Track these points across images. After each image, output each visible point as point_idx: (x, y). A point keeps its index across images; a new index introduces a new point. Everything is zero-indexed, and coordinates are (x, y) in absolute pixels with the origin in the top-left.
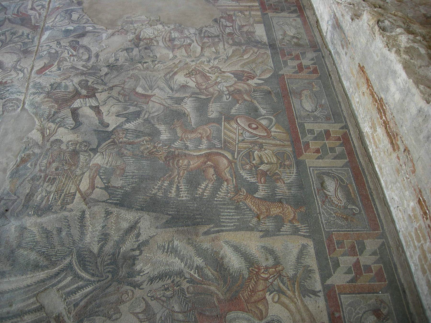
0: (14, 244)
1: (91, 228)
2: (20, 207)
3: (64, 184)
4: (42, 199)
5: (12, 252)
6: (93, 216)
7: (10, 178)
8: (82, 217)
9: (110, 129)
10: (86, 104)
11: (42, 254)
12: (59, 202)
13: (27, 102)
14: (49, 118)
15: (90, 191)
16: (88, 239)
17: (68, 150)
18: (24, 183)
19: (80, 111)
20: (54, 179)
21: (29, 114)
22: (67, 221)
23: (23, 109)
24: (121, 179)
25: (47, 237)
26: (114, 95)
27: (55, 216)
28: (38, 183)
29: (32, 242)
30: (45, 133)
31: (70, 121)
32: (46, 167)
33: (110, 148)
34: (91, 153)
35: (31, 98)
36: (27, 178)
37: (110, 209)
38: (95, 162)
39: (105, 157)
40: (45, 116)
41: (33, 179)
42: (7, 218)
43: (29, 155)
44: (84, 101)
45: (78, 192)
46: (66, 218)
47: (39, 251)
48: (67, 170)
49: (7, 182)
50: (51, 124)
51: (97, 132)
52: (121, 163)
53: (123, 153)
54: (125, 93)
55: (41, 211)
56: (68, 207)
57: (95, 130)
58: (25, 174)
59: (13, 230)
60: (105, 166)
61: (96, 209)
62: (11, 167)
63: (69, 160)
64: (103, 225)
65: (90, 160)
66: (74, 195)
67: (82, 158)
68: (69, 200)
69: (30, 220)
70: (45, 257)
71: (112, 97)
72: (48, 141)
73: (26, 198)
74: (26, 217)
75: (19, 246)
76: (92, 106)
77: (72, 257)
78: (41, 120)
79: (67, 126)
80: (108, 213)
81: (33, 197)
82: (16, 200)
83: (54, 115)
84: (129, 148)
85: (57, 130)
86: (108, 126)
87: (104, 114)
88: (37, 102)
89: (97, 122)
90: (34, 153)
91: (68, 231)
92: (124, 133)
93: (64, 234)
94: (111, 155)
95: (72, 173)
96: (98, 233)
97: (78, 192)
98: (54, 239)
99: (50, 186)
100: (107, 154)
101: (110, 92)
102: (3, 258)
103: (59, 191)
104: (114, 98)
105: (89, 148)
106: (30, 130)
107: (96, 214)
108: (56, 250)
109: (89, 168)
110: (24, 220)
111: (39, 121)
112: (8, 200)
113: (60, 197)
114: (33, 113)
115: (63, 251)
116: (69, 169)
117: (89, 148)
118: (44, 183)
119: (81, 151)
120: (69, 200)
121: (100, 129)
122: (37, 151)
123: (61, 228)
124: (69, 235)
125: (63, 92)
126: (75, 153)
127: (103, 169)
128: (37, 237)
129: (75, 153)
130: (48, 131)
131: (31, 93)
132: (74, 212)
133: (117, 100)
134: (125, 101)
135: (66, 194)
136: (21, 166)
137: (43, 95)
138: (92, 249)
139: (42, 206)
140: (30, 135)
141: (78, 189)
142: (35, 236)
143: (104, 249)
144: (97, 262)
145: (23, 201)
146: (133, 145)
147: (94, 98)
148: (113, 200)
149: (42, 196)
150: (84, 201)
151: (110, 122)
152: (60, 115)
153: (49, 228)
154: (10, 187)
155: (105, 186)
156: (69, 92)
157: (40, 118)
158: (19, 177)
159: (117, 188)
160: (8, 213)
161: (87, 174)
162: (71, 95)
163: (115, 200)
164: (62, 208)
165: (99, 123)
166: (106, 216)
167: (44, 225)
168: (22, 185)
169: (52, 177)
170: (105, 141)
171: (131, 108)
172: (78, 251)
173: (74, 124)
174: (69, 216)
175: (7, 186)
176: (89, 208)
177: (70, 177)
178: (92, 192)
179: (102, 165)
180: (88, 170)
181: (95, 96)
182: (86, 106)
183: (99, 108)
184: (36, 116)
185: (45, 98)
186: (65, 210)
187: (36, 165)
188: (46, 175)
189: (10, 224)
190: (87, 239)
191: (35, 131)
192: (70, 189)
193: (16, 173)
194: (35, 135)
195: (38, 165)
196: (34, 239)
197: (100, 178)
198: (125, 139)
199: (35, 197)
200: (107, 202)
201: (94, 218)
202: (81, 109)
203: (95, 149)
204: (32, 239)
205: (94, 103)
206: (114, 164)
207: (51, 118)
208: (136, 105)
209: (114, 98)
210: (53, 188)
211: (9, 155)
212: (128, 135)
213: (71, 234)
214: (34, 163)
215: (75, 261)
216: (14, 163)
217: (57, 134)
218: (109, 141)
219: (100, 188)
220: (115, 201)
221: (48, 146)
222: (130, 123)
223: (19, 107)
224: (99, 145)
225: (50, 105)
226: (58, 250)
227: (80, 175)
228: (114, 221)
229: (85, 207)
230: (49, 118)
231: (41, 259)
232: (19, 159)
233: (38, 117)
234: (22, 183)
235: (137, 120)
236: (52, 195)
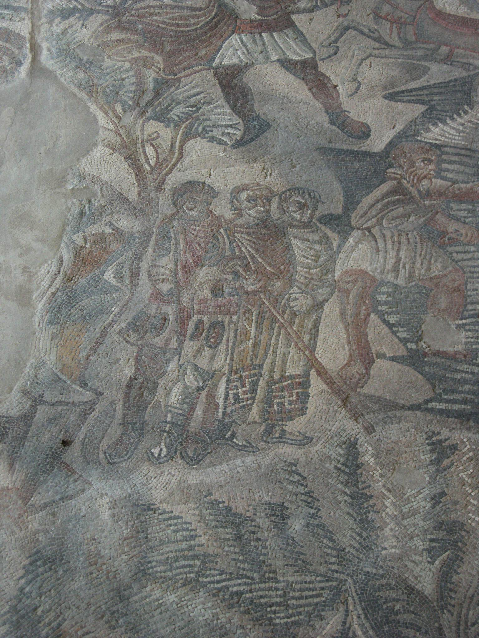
0: (122, 565)
1: (393, 504)
2: (115, 431)
3: (255, 345)
4: (190, 399)
5: (121, 595)
6: (390, 459)
7: (51, 322)
8: (352, 466)
9: (378, 143)
10: (264, 52)
11: (234, 600)
12: (255, 409)
13: (45, 45)
14: (143, 103)
15: (357, 369)
16: (389, 544)
17: (240, 221)
18: (108, 341)
19: (249, 79)
20: (217, 327)
21: (62, 88)
22: (296, 478)
23: (36, 69)
24: (459, 327)
25: (238, 537)
26: (358, 19)
27: (249, 460)
28: (159, 341)
29: (185, 558)
30: (142, 159)
31: (222, 114)
32: (177, 283)
33: (394, 213)
34: (330, 233)
35: (57, 29)
36: (113, 322)
37: (445, 433)
38: (351, 264)
39: (381, 245)
40: (127, 95)
41: (137, 326)
42: (74, 473)
43: (100, 239)
44: (254, 41)
45: (313, 372)
46: (291, 467)
47: (220, 590)
48: (255, 293)
49: (43, 339)
50: (153, 127)
51: (335, 156)
52: (444, 267)
53: (443, 234)
54: (399, 14)
55: (197, 442)
56: (295, 426)
57: (323, 150)
58: (103, 310)
59: (106, 514)
60: (390, 277)
61: (393, 432)
62: (45, 283)
63: (253, 257)
64: (434, 491)
65: (332, 259)
66: (305, 384)
67: (300, 248)
68: (290, 403)
69: (163, 479)
70: (247, 612)
71: (355, 28)
72: (159, 188)
73: (127, 396)
74: (145, 467)
75: (142, 573)
76: (290, 61)
77: (347, 611)
78: (114, 111)
79: (216, 133)
80: (442, 451)
81: (153, 391)
82: (91, 405)
83: (157, 94)
84: (463, 214)
85: (181, 147)
86: (365, 133)
87: (340, 88)
88: (81, 45)
89: (323, 119)
90: (116, 230)
91: (313, 516)
92: (430, 161)
93: (298, 527)
94: (403, 239)
95: (275, 302)
96: (421, 523)
97: (313, 372)
98: (265, 547)
99: (207, 352)
100: (388, 234)
101: (344, 10)
102: (91, 619)
103: (246, 370)
104: (362, 32)
105: (317, 214)
106: (84, 148)
107: (399, 454)
108: (281, 585)
109: (334, 285)
110: (137, 478)
111: (107, 113)
112: (60, 403)
113: (254, 391)
114: (79, 86)
115: (310, 589)
116: (264, 289)
117: (317, 214)
118: (181, 343)
119: (291, 225)
120: (290, 403)
121: (338, 146)
122: (125, 223)
123: (282, 506)
124: (317, 528)
125: (172, 7)
126: (270, 233)
127: (384, 289)
128: (203, 540)
129: (270, 233)
130: (150, 151)
131: (52, 12)
132: (318, 447)
133: (375, 39)
134: (407, 44)
135: (271, 382)
136: (82, 281)
137: (101, 18)
138: (412, 581)
139: (194, 426)
140: (86, 165)
141: (313, 363)
142: (193, 537)
143: (455, 578)
144: (440, 629)
145: (119, 407)
146: (472, 202)
147: (289, 31)
148: (447, 401)
149: (186, 387)
150: (345, 405)
151: (369, 120)
152: (180, 93)
153: (239, 506)
154: (60, 358)
155: (410, 350)
156: (193, 9)
157: (108, 103)
158: (84, 318)
159: (453, 357)
160: (73, 454)
161: (331, 309)
162: (203, 20)
163: (455, 402)
164: (269, 432)
165: (332, 123)
166: (438, 461)
167: (216, 496)
168: (102, 348)
169: (205, 318)
170: (370, 189)
171: (434, 68)
172: (363, 589)
173: (242, 128)
174: (303, 459)
175: (45, 352)
176: (369, 430)
177: (274, 320)
178: (368, 373)
179: (378, 277)
180: (331, 294)
181: (291, 25)
182: (267, 58)
183: (315, 67)
184: (90, 94)
185: (109, 29)
186: (282, 438)
187: (135, 275)
188: (181, 311)
189: (88, 493)
190: (386, 545)
191: (100, 152)
192: (284, 362)
193: (70, 302)
194: (106, 166)
195: (144, 277)
196: (191, 548)
197: (384, 321)
198: (438, 182)
199: (160, 391)
200: (431, 411)
201: (394, 467)
202: (252, 70)
203: (338, 217)
204: (184, 545)
205: (297, 53)
206: (420, 270)
207: (150, 103)
208: (448, 59)
209: (362, 32)
210: (221, 361)
211: (27, 238)
212: (445, 166)
213: (322, 526)
214: (127, 266)
215: (362, 625)
216: (54, 269)
217: (186, 161)
218: (385, 187)
219: (394, 359)
220: (456, 407)
221: (165, 206)
222: (444, 123)
223: (19, 64)
224: (350, 203)
225: (136, 54)
226: (289, 585)
227: (309, 313)
228: (470, 476)
229: (353, 428)
230: (143, 103)
231: (235, 620)
232: (67, 256)
233: (101, 101)
234: (99, 343)
235: (466, 113)
236: (222, 386)
